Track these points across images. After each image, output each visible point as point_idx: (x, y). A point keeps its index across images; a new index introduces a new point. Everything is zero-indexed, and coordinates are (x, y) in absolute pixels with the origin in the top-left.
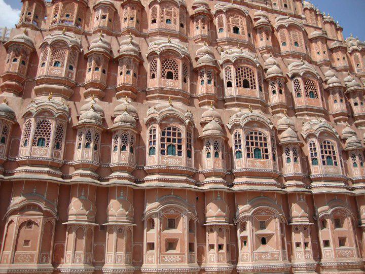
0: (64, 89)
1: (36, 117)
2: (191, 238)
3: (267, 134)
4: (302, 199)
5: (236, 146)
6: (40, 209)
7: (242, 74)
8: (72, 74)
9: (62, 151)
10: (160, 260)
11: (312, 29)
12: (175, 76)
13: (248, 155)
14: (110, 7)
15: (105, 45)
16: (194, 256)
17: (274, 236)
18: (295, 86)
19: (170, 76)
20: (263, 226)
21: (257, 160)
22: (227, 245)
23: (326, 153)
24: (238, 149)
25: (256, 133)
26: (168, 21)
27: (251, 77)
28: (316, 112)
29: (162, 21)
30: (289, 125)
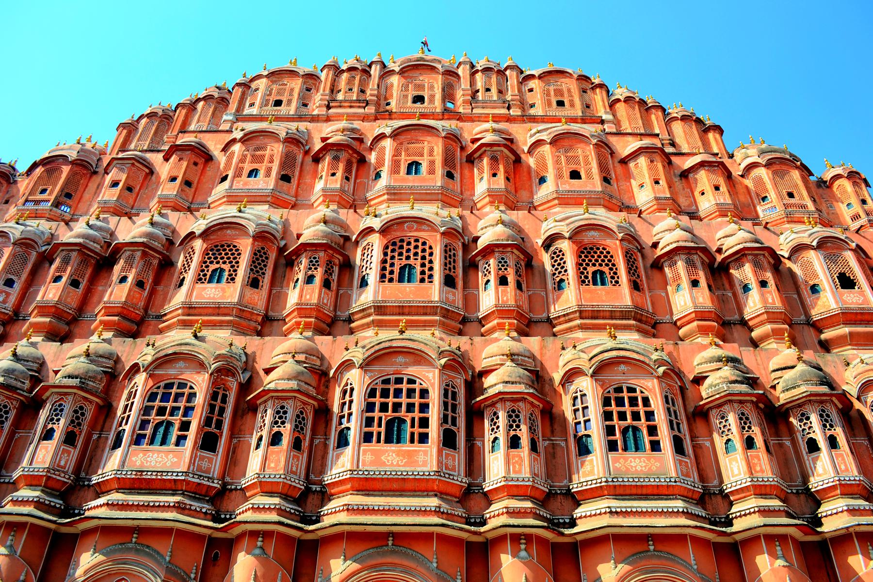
3: (430, 378)
4: (523, 554)
7: (401, 254)
11: (630, 138)
12: (230, 275)
13: (367, 438)
14: (133, 164)
18: (553, 266)
19: (216, 276)
21: (393, 447)
23: (622, 416)
26: (253, 173)
27: (423, 258)
28: (612, 318)
29: (240, 175)
30: (512, 356)
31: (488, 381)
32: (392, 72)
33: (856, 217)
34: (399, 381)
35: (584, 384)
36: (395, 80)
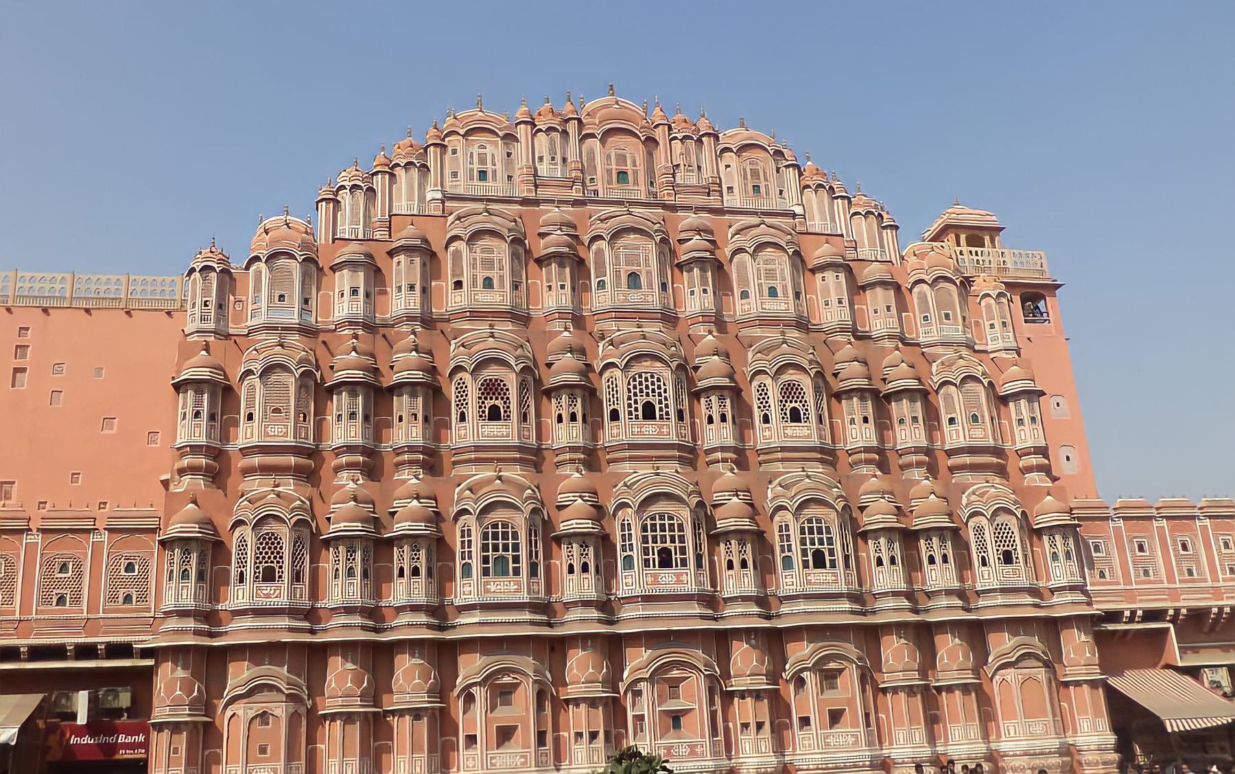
2: (539, 720)
5: (624, 549)
6: (279, 690)
7: (641, 391)
9: (304, 587)
22: (607, 733)
24: (629, 553)
25: (662, 518)
26: (488, 283)
27: (660, 394)
31: (718, 513)
32: (592, 136)
33: (995, 339)
36: (595, 143)
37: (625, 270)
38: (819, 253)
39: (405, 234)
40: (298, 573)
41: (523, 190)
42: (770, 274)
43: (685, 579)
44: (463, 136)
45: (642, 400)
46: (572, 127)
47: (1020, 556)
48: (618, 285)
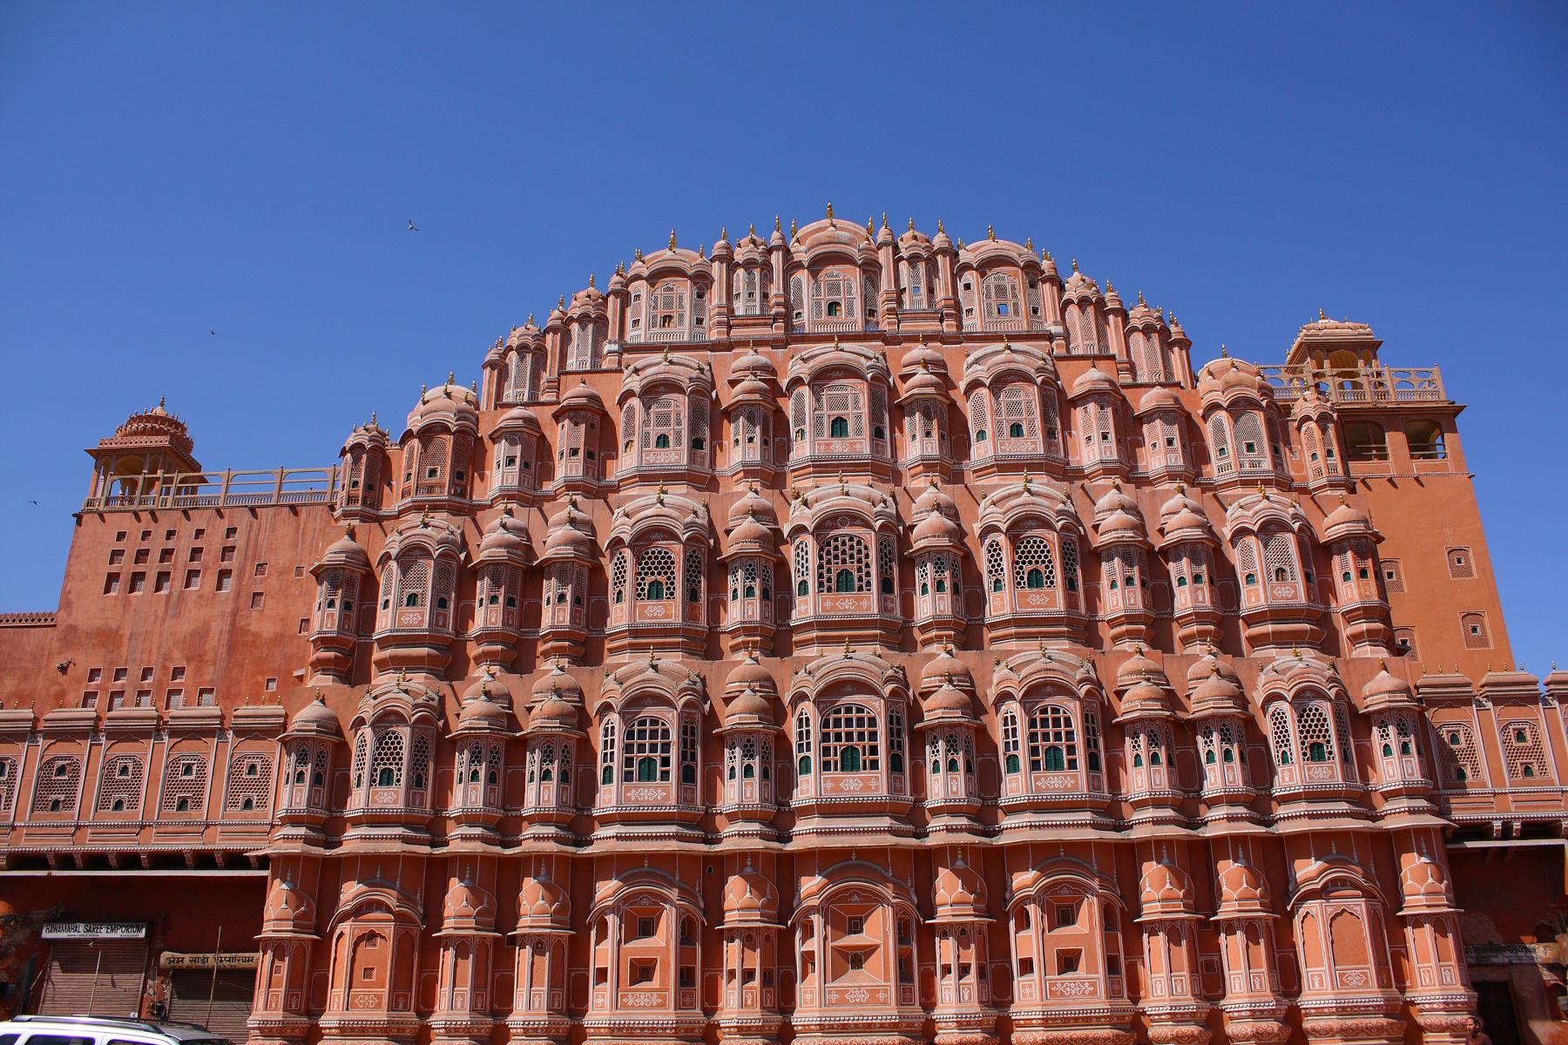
0: (429, 655)
1: (372, 726)
4: (960, 863)
6: (389, 910)
7: (836, 557)
8: (445, 616)
10: (616, 1005)
11: (1082, 363)
13: (826, 766)
15: (511, 537)
16: (692, 995)
17: (879, 953)
20: (856, 928)
23: (1046, 737)
25: (848, 710)
26: (663, 441)
27: (859, 561)
32: (799, 265)
34: (848, 710)
35: (1013, 707)
36: (803, 276)
37: (828, 414)
38: (1082, 379)
39: (574, 391)
40: (419, 778)
41: (714, 335)
42: (1013, 408)
43: (873, 783)
44: (647, 279)
45: (836, 568)
46: (776, 259)
47: (1335, 750)
48: (820, 434)
